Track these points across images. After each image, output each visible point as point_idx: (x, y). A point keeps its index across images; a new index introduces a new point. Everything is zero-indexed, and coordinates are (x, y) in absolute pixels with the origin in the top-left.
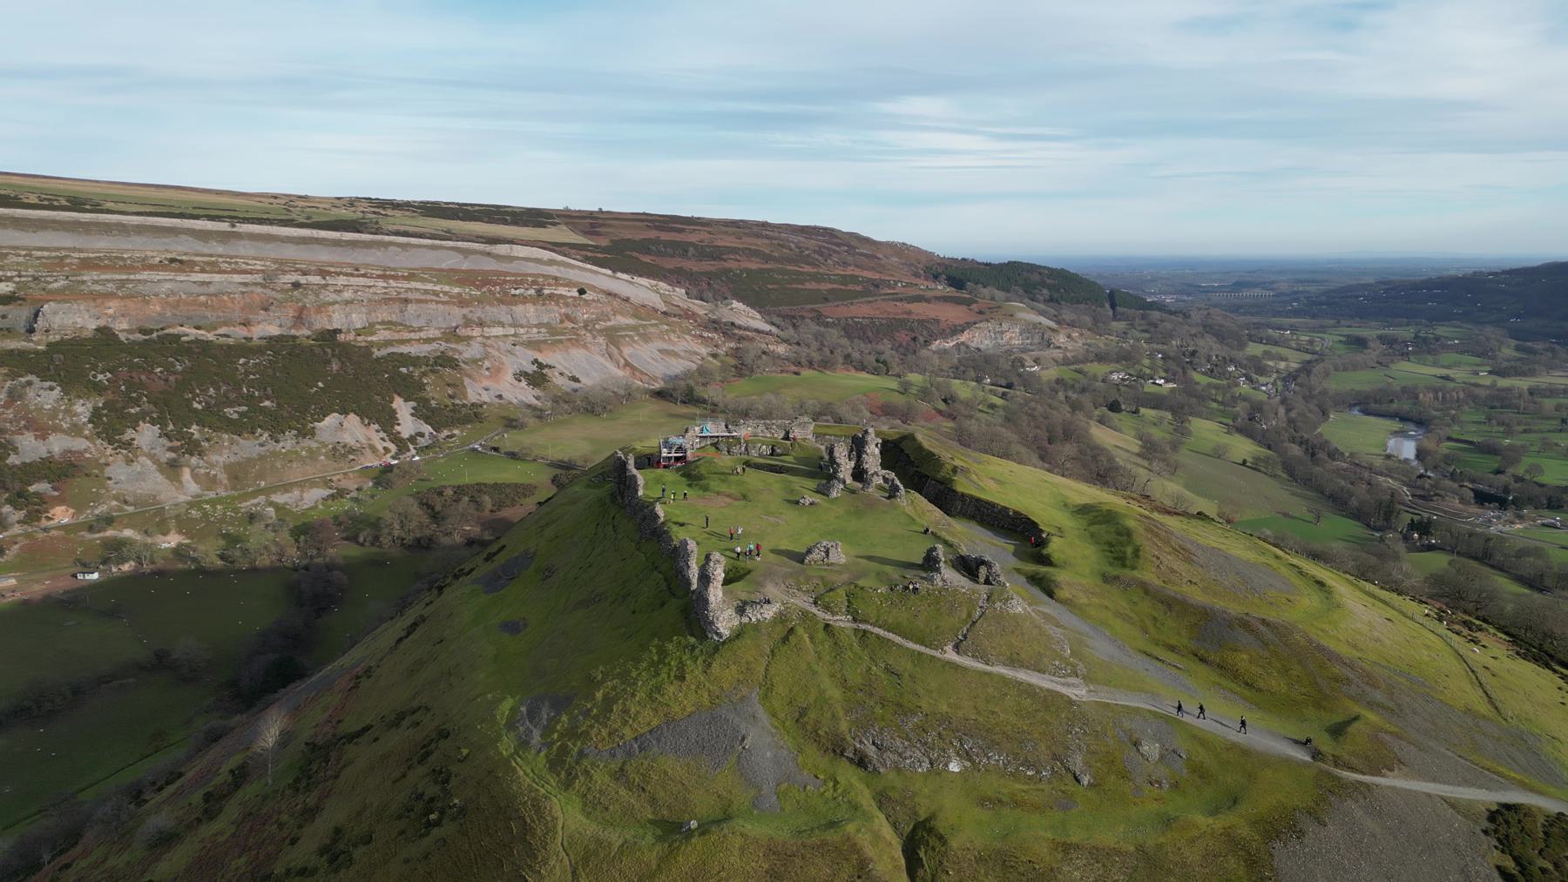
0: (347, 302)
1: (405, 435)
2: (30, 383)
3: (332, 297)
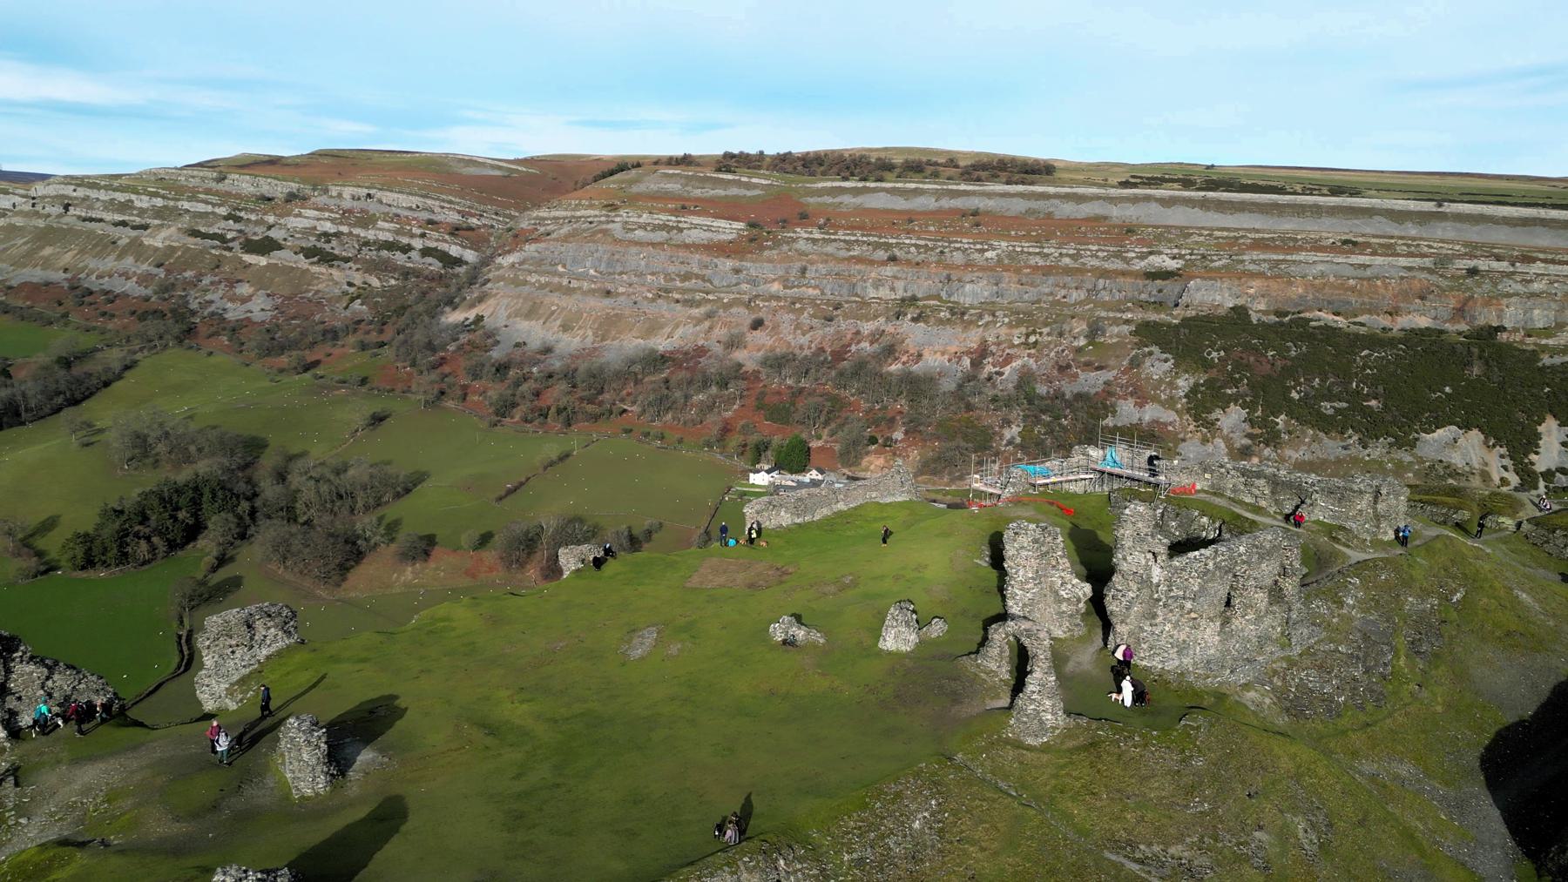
0: (1533, 295)
1: (1540, 467)
2: (1151, 353)
3: (1519, 288)
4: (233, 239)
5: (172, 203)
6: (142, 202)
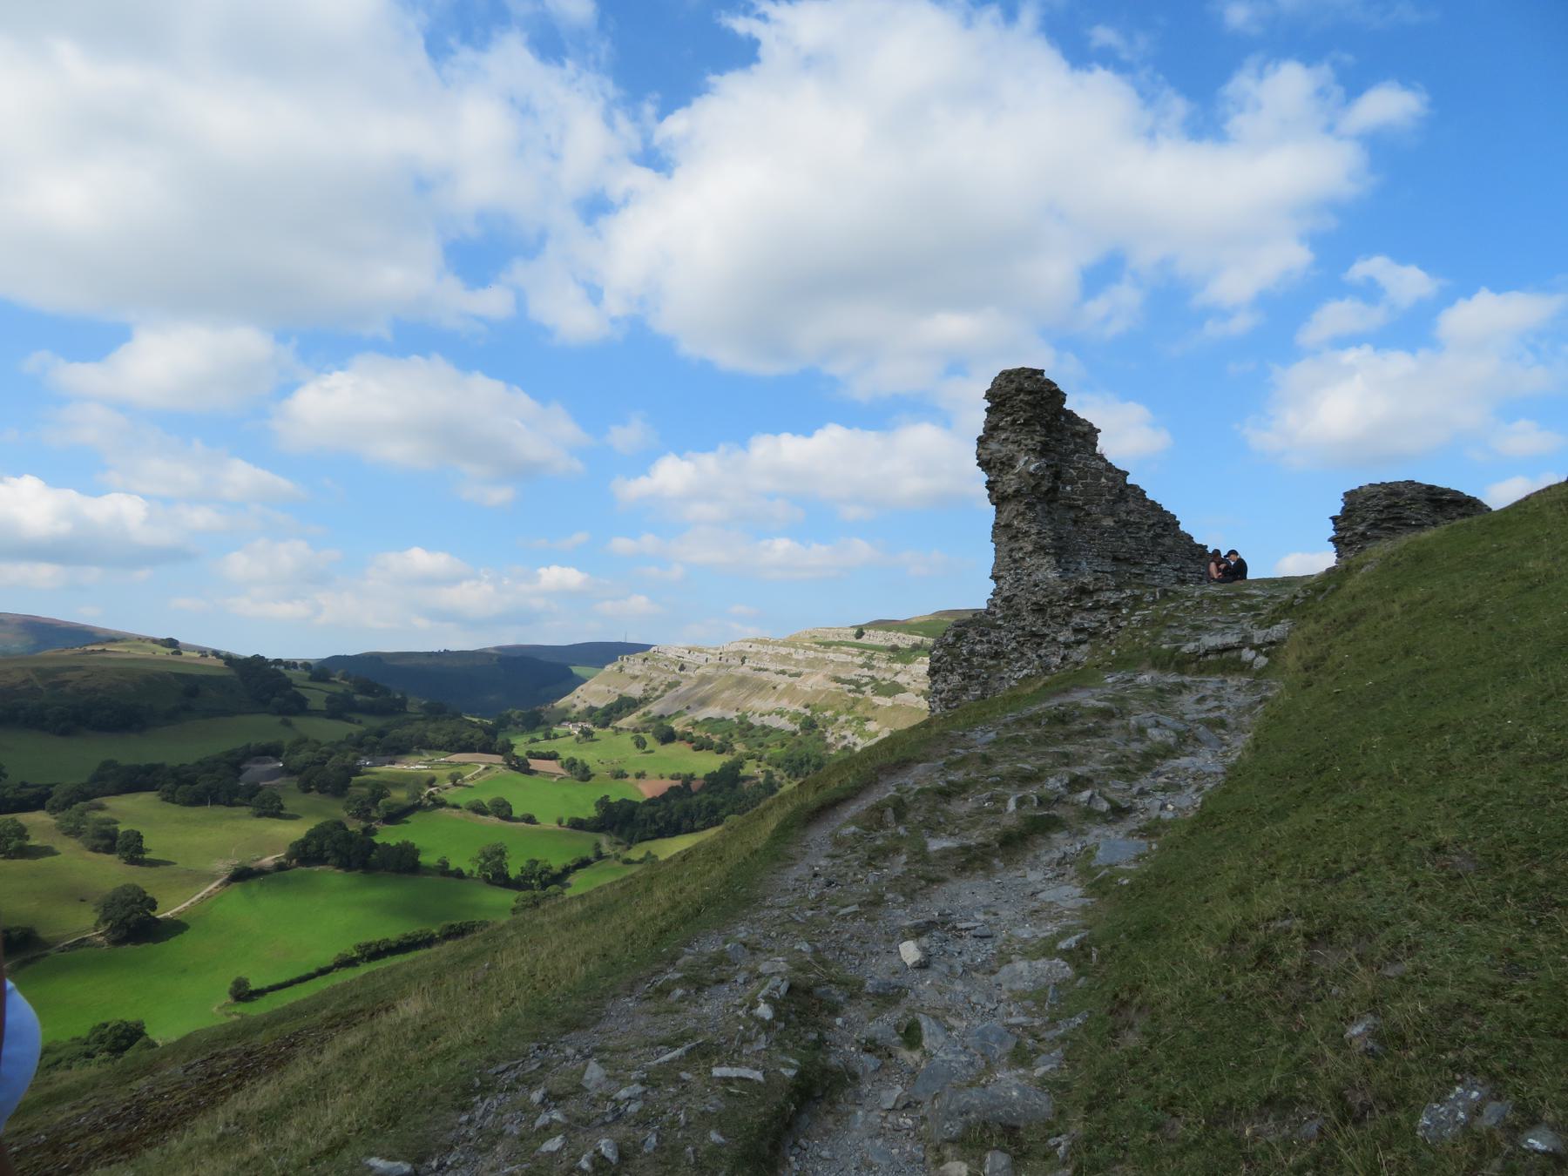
6: (800, 655)
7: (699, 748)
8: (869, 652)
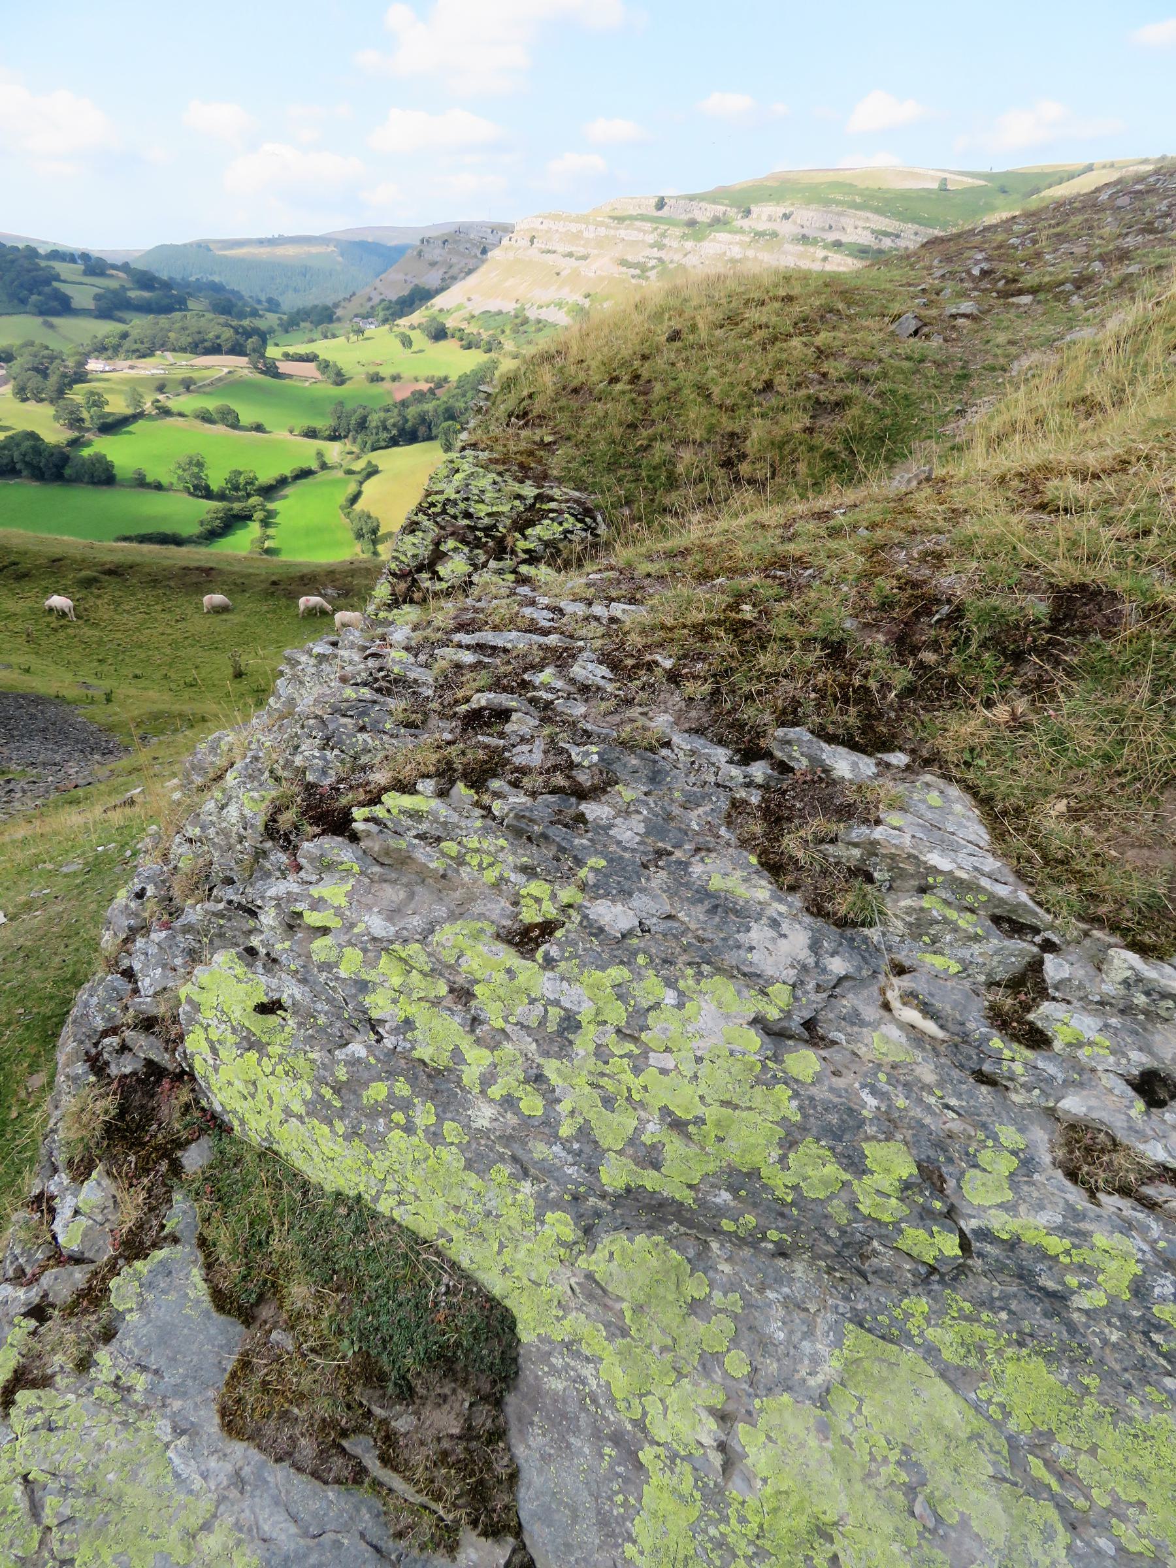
4: (653, 267)
5: (612, 232)
6: (590, 234)
7: (469, 347)
8: (663, 227)
